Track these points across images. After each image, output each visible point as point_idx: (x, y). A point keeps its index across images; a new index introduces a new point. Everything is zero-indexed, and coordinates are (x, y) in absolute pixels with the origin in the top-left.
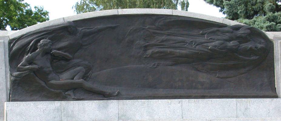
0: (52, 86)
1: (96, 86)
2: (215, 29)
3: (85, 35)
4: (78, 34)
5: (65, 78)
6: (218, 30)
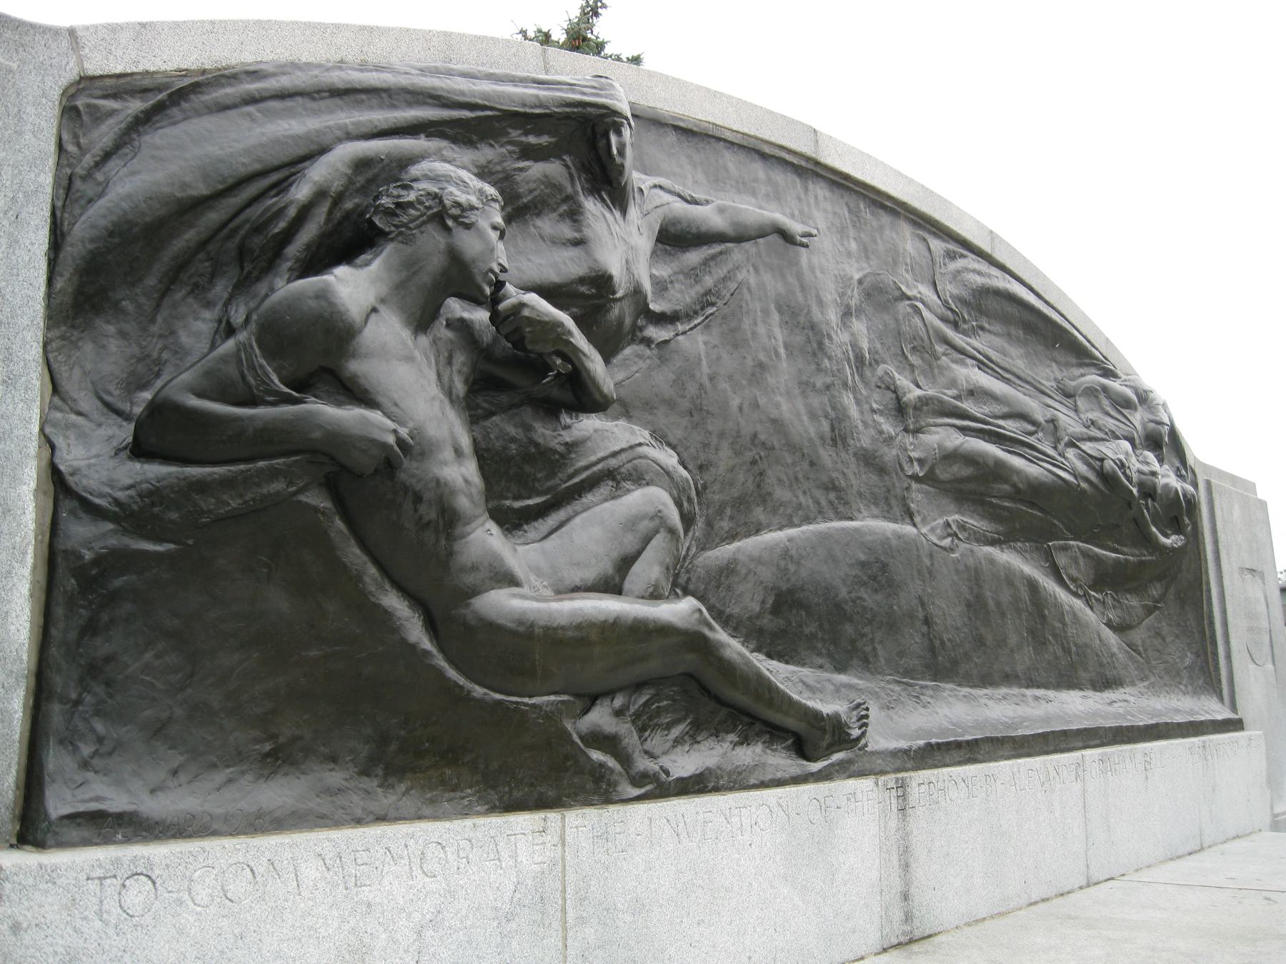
4: (633, 212)
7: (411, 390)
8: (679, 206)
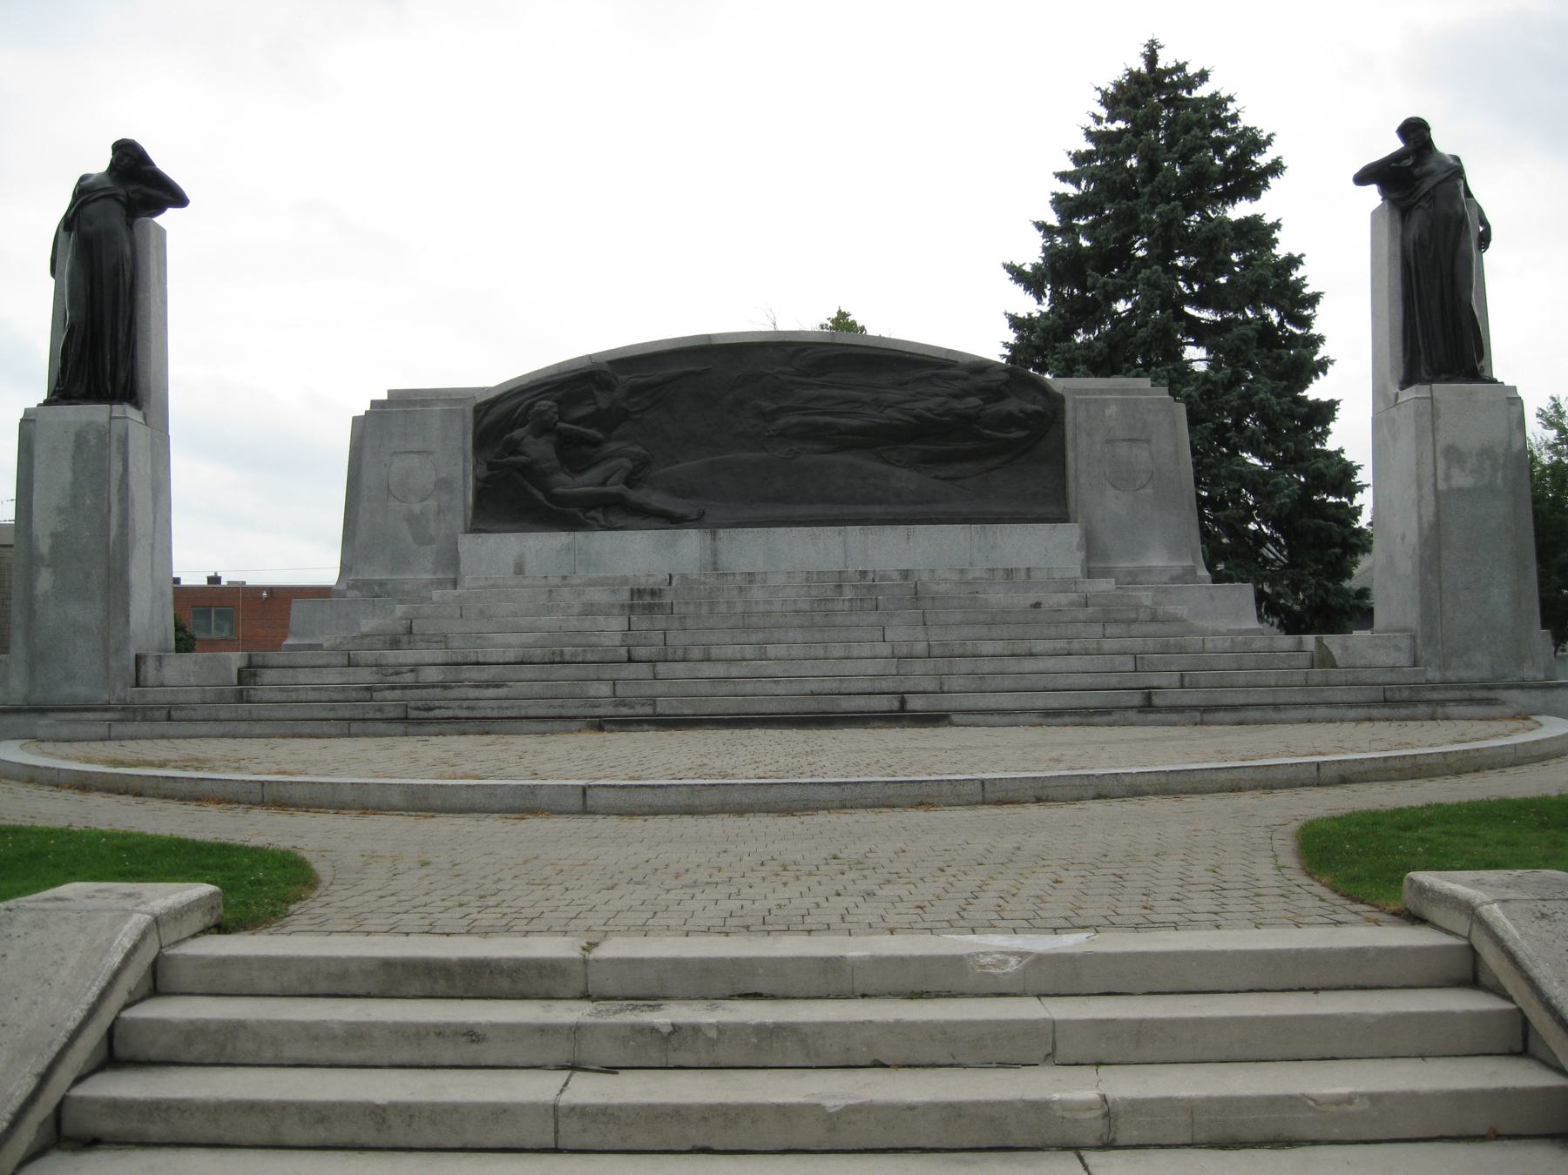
1: (656, 500)
2: (929, 372)
3: (635, 390)
5: (569, 484)
7: (539, 449)
8: (642, 380)
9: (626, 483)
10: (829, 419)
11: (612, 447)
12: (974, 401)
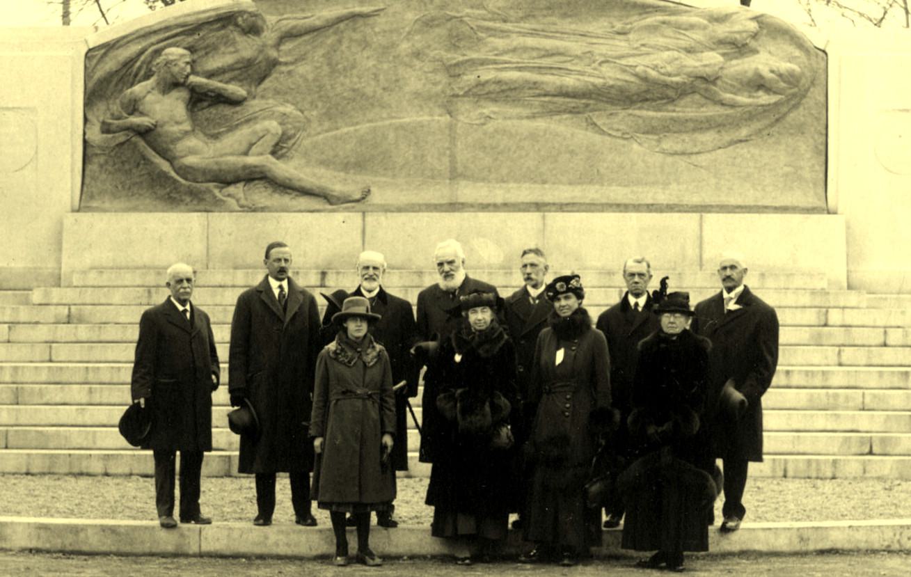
0: (185, 171)
4: (265, 34)
6: (664, 23)
7: (166, 109)
9: (273, 153)
10: (528, 75)
11: (255, 105)
12: (712, 59)
